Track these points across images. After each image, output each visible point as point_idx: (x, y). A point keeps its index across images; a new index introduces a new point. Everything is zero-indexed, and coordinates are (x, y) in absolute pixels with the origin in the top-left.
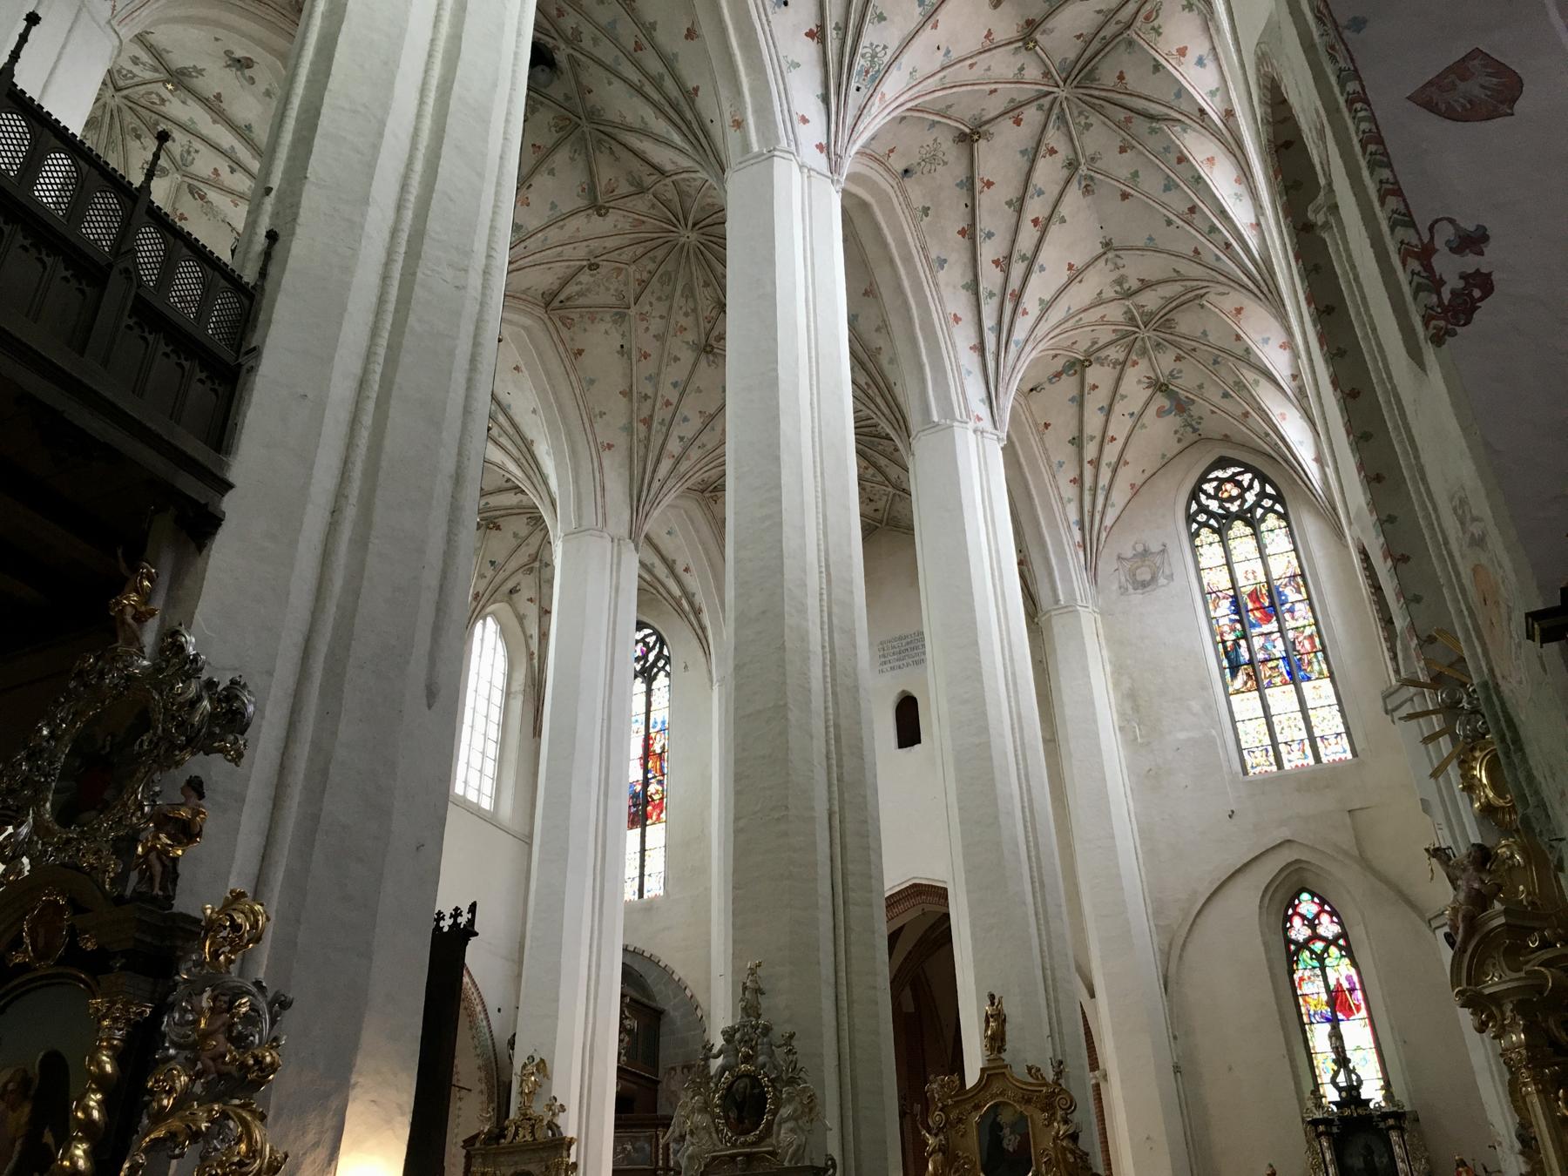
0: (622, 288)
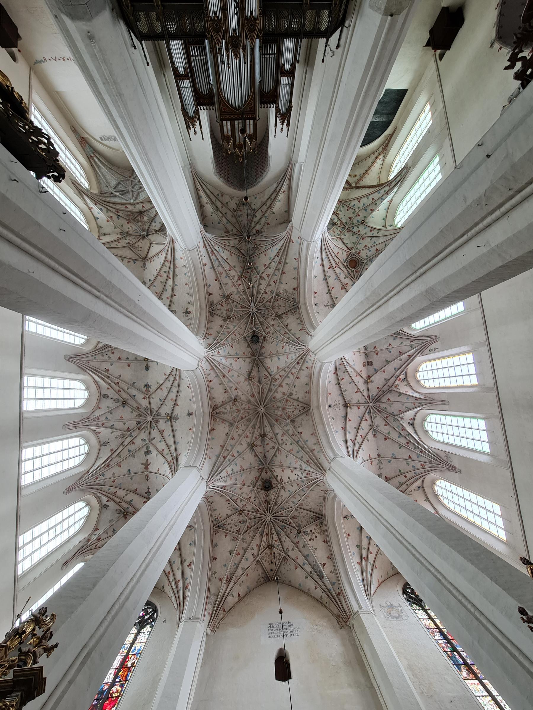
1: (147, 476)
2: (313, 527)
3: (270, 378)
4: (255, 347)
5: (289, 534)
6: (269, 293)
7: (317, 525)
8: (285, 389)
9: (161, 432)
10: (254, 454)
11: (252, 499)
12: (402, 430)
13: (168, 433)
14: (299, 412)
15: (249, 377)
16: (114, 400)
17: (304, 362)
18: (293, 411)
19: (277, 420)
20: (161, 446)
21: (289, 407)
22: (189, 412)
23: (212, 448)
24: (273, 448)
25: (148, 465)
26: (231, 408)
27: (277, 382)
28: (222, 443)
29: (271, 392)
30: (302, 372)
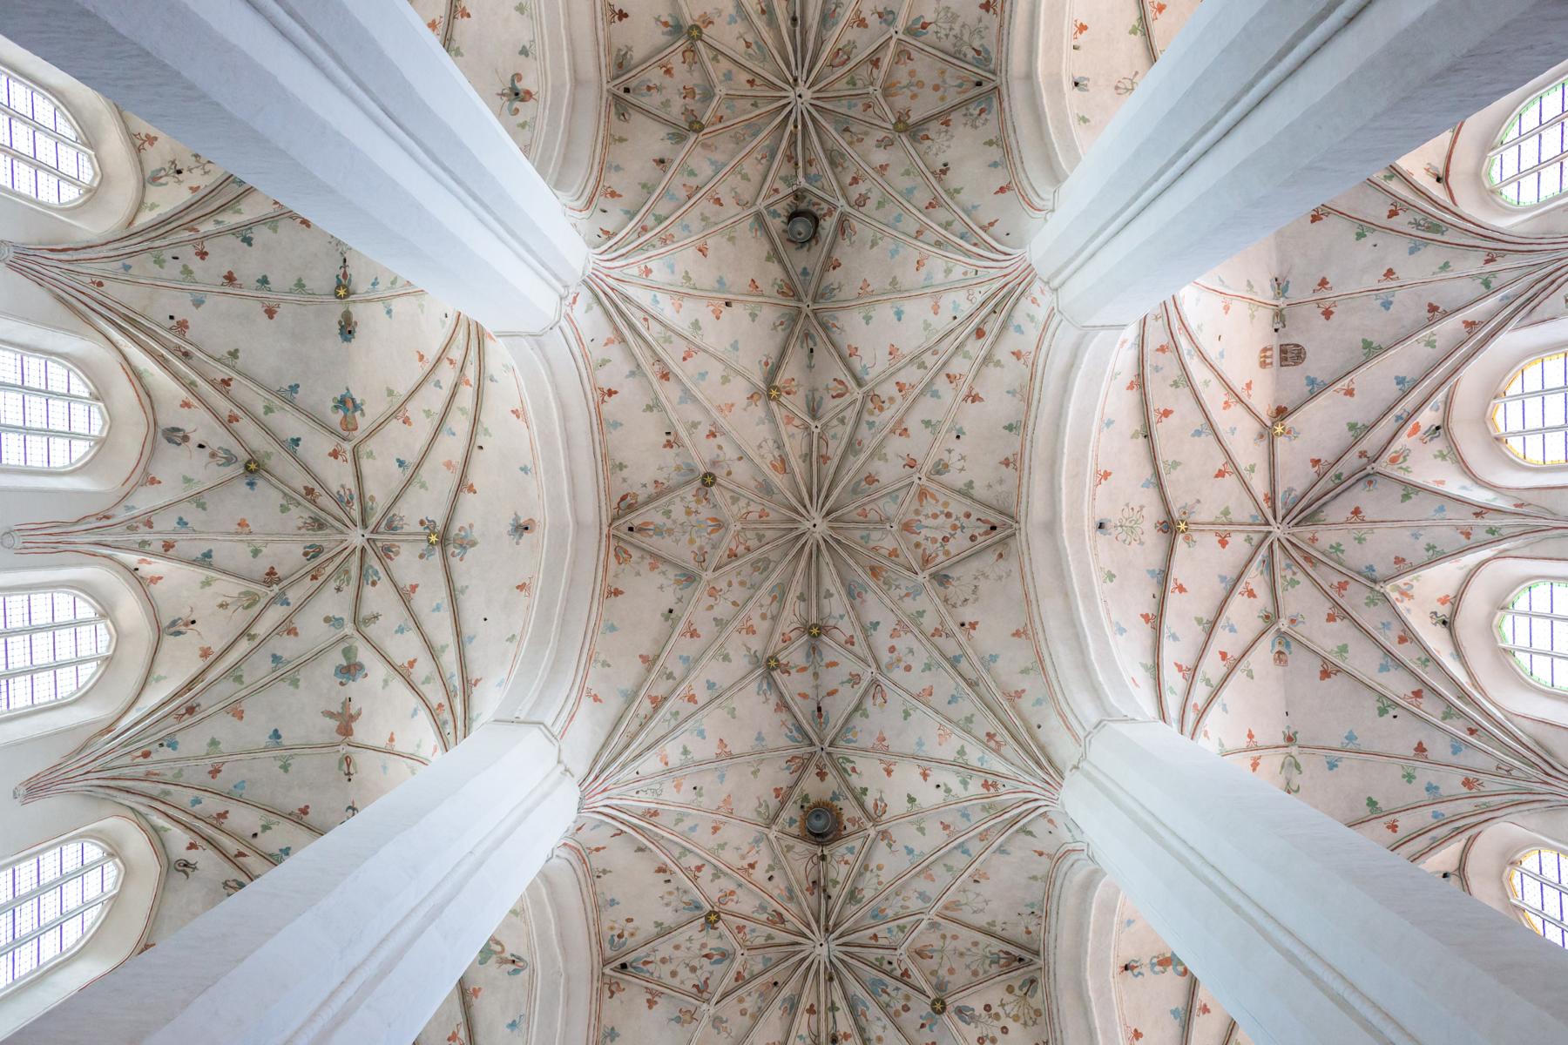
0: (707, 548)
1: (347, 760)
2: (994, 994)
3: (858, 393)
4: (800, 259)
5: (897, 1013)
6: (873, 20)
7: (1010, 989)
8: (917, 443)
9: (405, 596)
10: (773, 699)
11: (759, 874)
12: (1402, 640)
13: (429, 598)
14: (969, 543)
15: (770, 390)
16: (213, 455)
17: (1004, 327)
18: (945, 539)
19: (874, 572)
20: (406, 647)
21: (930, 522)
22: (517, 518)
23: (605, 664)
24: (855, 679)
25: (353, 718)
26: (689, 512)
27: (887, 414)
28: (648, 648)
29: (856, 453)
30: (991, 371)
